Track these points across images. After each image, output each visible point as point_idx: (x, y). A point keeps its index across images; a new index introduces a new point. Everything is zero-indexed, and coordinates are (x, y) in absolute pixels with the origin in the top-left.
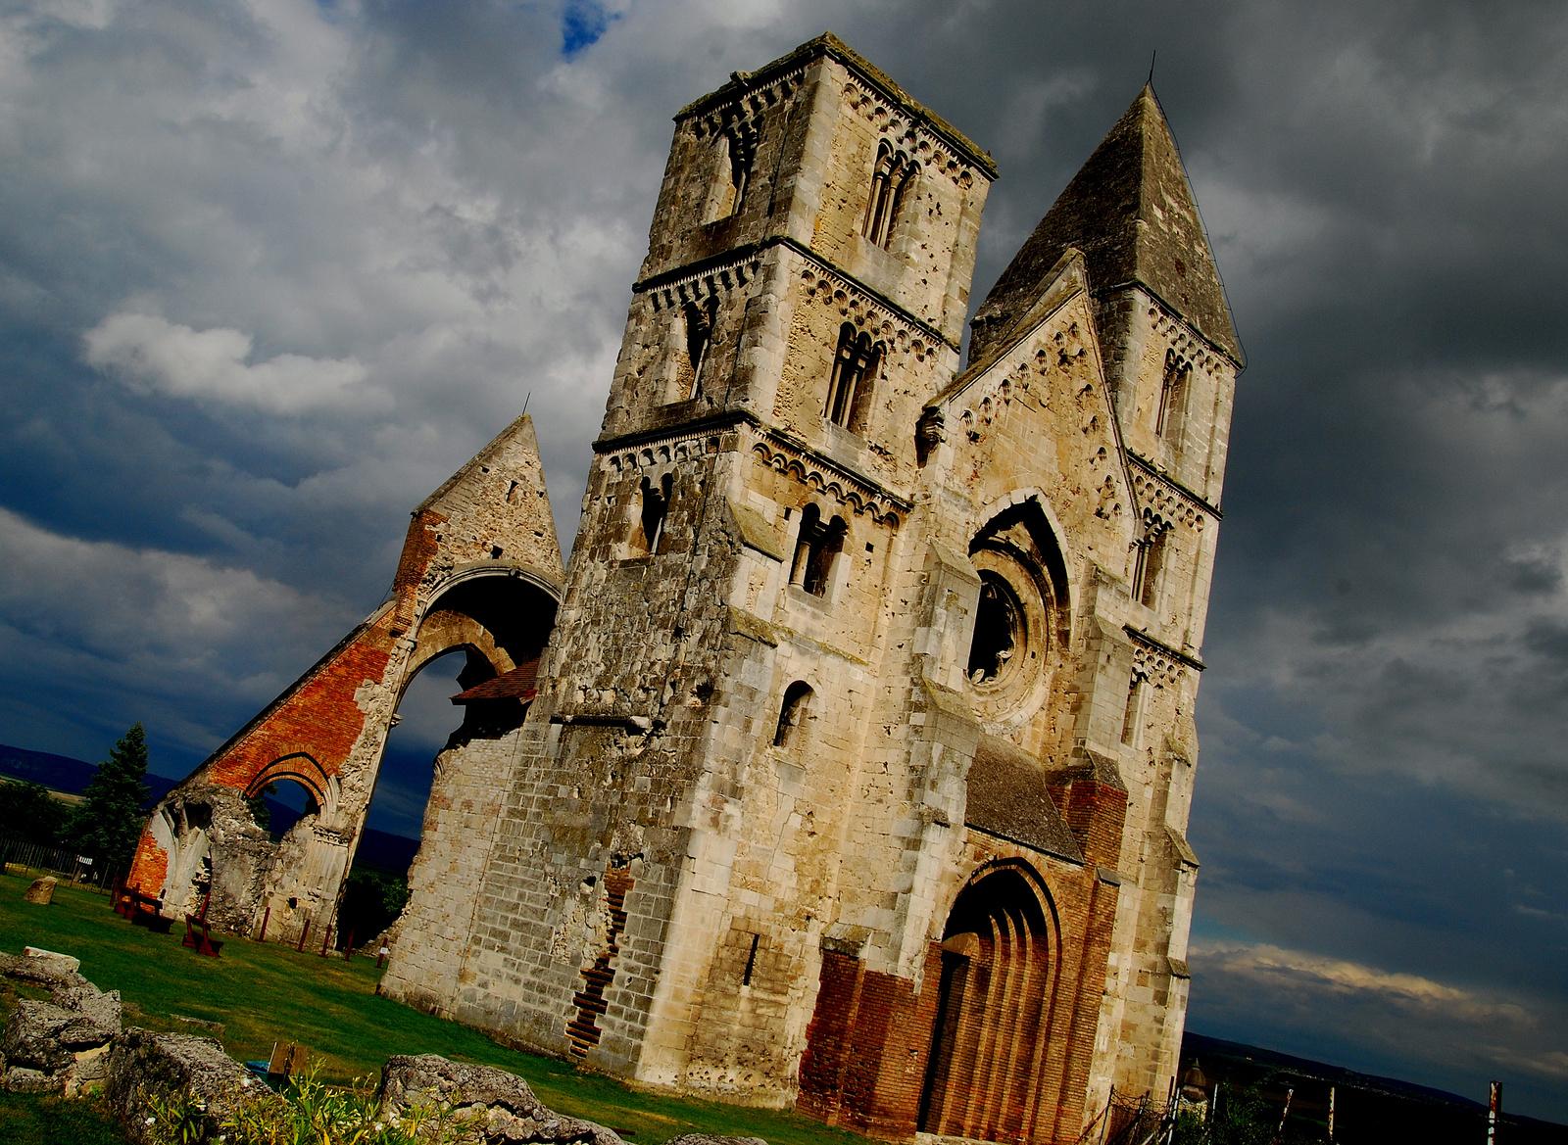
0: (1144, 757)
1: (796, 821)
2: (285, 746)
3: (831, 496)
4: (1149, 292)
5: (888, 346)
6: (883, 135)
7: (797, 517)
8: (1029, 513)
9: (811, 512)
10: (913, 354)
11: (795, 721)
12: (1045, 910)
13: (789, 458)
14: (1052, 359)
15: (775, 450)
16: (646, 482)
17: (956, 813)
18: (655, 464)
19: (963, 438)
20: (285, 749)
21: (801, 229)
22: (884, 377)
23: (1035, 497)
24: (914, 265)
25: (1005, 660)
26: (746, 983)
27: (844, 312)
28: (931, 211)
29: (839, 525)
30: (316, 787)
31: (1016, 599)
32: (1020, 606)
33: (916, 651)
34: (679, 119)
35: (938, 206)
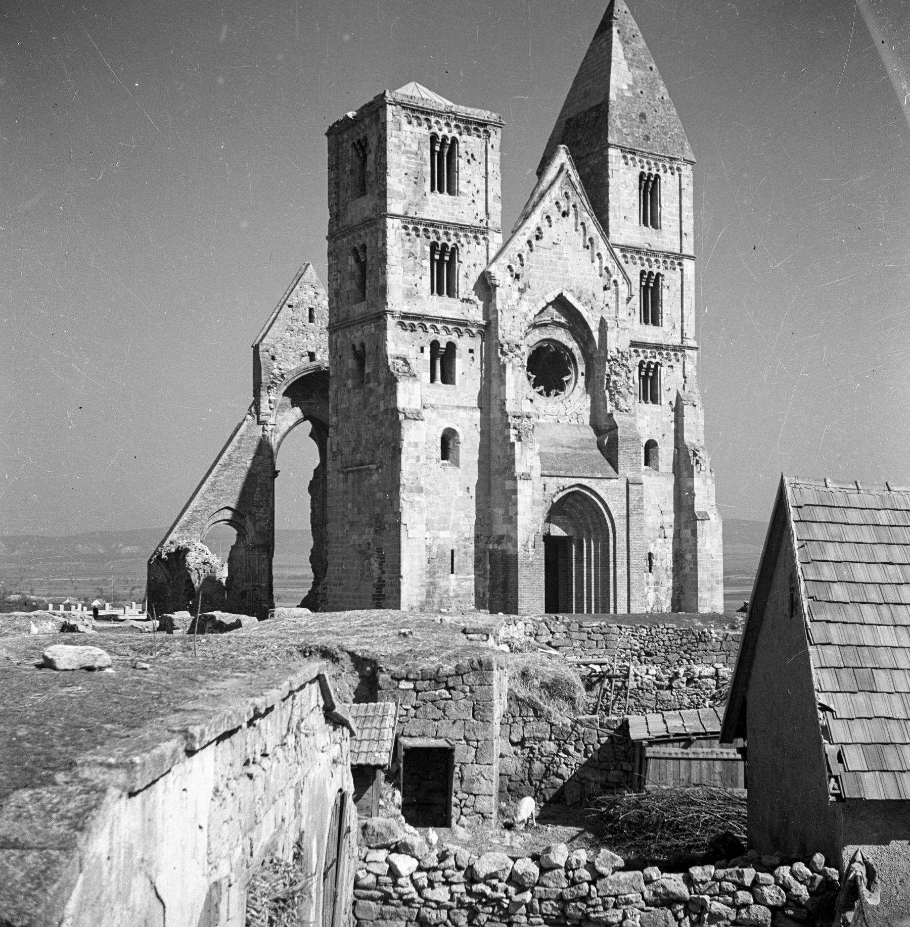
0: (669, 408)
1: (461, 493)
2: (215, 506)
3: (443, 333)
4: (617, 146)
5: (459, 245)
6: (431, 131)
7: (427, 350)
8: (561, 303)
9: (435, 345)
10: (474, 242)
11: (451, 446)
12: (601, 506)
13: (416, 323)
14: (555, 215)
15: (407, 322)
16: (354, 347)
17: (536, 473)
18: (357, 336)
19: (510, 280)
20: (215, 508)
21: (394, 206)
22: (459, 261)
23: (561, 295)
24: (465, 195)
25: (567, 381)
26: (452, 572)
27: (428, 238)
28: (469, 161)
29: (451, 346)
30: (239, 525)
31: (566, 348)
32: (570, 351)
33: (502, 398)
34: (328, 134)
35: (472, 156)
